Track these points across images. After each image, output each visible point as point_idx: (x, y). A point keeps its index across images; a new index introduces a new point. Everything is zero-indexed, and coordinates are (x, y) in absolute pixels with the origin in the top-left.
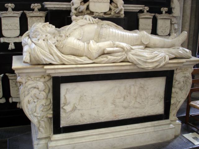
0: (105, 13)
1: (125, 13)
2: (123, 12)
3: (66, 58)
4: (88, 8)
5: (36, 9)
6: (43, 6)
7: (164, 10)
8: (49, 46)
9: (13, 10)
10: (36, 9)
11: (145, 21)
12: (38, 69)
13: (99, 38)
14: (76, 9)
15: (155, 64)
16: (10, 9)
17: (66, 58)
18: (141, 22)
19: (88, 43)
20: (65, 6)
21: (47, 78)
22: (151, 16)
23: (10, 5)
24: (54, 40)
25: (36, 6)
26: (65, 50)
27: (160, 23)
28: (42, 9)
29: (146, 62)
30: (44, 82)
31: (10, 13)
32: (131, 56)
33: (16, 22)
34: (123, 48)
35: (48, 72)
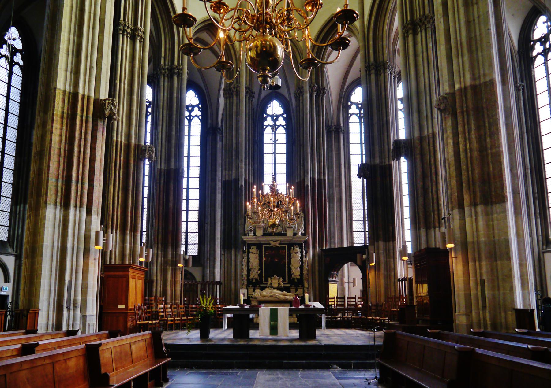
11: (293, 289)
13: (271, 293)
25: (258, 286)
27: (299, 290)
28: (260, 287)
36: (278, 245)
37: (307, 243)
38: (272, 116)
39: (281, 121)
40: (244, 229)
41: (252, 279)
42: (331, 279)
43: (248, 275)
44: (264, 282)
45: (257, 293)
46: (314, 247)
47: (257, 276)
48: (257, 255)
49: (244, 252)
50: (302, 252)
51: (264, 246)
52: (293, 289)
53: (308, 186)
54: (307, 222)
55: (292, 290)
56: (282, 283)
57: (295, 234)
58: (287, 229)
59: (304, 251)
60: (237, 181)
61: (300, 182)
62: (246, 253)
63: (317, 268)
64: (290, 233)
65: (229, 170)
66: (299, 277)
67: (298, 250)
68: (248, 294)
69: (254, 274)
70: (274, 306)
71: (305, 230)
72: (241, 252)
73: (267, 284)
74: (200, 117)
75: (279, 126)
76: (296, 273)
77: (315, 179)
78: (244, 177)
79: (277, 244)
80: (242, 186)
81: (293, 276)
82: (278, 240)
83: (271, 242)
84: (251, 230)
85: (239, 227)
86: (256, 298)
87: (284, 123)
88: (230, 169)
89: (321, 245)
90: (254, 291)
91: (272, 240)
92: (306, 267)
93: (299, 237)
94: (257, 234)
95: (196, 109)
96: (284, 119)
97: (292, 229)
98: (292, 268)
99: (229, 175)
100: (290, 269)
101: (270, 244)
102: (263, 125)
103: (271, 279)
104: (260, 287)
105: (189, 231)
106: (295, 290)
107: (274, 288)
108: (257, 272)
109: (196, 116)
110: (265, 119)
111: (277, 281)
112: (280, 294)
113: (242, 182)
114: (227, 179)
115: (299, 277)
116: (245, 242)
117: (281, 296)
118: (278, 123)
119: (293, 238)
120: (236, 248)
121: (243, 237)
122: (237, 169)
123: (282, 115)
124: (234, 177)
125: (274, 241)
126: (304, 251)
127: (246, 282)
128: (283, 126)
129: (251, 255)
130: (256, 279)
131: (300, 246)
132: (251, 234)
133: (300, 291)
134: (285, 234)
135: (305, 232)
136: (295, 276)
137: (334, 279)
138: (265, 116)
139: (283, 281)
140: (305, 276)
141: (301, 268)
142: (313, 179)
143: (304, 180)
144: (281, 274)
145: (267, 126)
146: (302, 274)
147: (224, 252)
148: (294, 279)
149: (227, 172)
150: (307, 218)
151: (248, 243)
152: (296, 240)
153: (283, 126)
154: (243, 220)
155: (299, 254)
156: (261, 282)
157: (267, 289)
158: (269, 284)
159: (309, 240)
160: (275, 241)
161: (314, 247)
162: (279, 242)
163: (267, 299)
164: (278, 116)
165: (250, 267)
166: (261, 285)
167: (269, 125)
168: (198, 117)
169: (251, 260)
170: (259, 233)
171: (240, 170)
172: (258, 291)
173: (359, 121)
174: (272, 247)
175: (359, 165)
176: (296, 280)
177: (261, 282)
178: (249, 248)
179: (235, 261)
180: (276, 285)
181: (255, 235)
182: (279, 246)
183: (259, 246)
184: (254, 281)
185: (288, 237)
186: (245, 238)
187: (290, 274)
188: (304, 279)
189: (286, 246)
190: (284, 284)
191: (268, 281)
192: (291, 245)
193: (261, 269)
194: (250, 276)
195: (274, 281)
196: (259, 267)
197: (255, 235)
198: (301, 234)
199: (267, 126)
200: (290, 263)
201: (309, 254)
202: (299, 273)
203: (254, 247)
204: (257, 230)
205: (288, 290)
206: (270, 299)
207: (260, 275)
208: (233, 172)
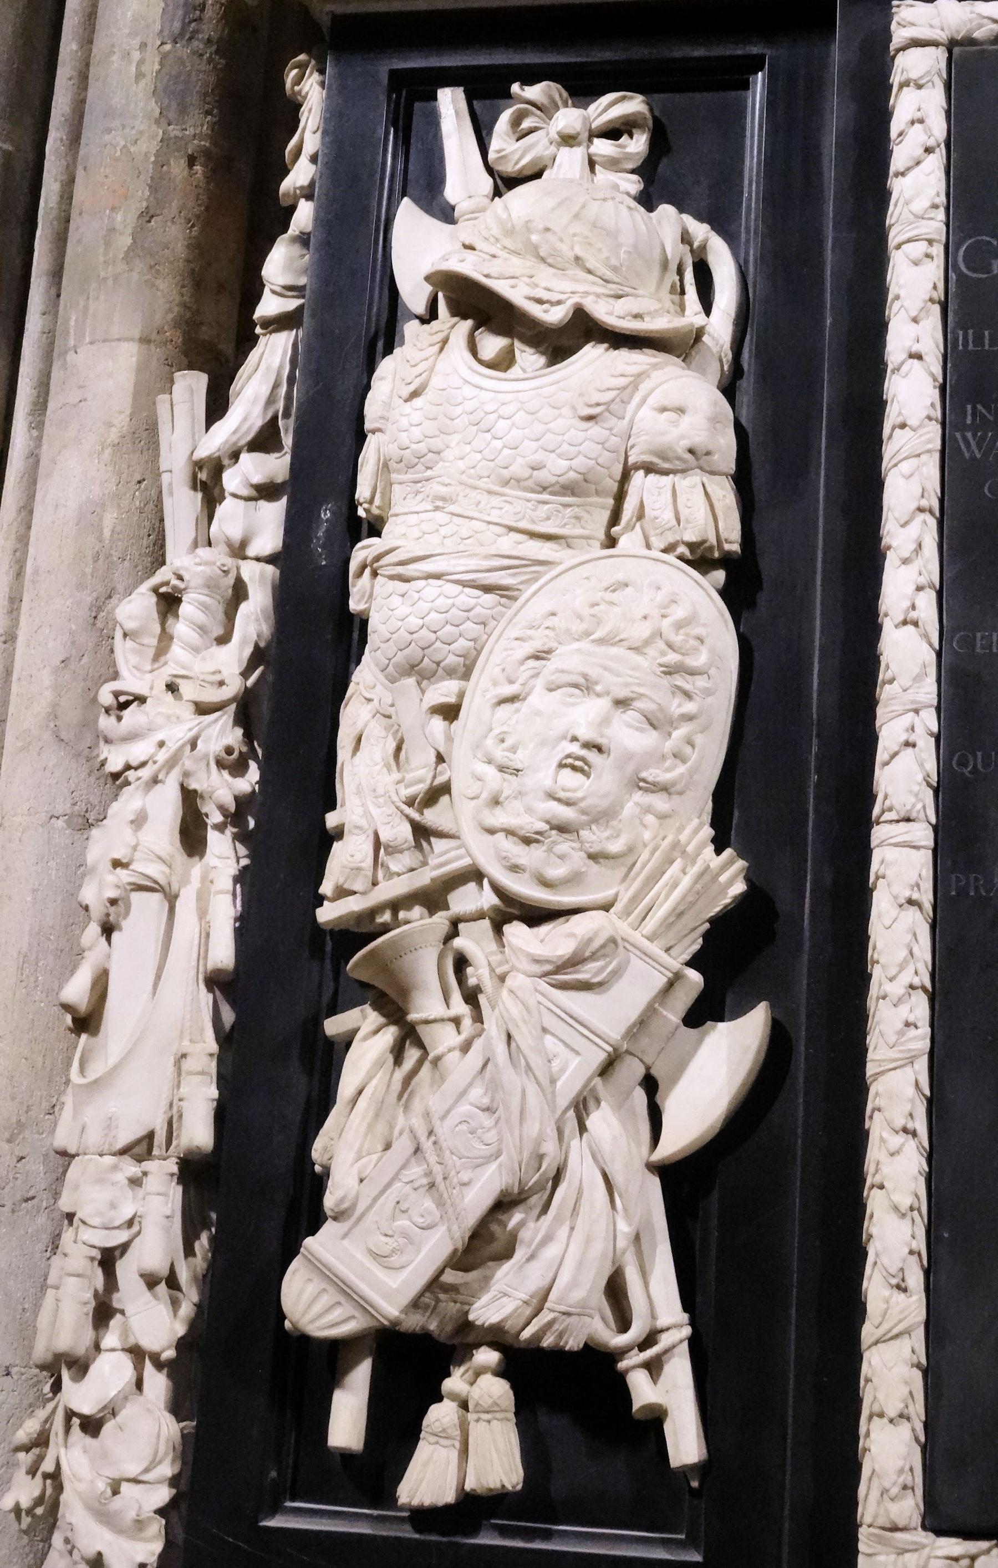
41: (411, 1365)
43: (255, 1189)
47: (599, 1261)
48: (686, 408)
49: (212, 343)
130: (567, 1389)
165: (350, 881)
193: (777, 947)
194: (302, 1204)
207: (762, 1211)
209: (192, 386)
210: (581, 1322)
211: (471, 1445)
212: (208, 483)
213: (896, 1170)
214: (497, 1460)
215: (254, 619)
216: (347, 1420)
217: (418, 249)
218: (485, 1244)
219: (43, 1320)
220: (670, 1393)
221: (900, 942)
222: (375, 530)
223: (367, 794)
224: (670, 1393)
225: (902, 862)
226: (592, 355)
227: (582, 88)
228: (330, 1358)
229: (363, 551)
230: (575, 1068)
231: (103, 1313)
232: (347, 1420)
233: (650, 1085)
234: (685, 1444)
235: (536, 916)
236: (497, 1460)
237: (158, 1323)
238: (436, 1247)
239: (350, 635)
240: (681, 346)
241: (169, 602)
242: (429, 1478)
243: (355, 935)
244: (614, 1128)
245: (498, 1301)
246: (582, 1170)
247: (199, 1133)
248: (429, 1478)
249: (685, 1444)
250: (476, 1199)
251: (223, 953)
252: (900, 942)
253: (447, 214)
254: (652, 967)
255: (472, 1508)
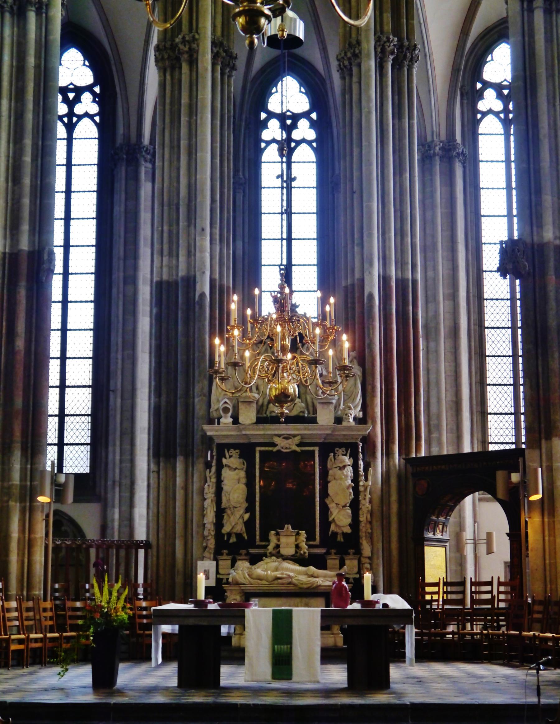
0: (293, 556)
1: (309, 554)
2: (307, 554)
3: (252, 581)
4: (279, 552)
5: (243, 554)
6: (248, 551)
7: (352, 551)
8: (244, 574)
9: (227, 554)
10: (243, 554)
11: (333, 561)
12: (237, 588)
13: (277, 569)
14: (270, 553)
15: (309, 585)
16: (225, 554)
17: (252, 581)
18: (329, 562)
19: (267, 572)
20: (263, 551)
21: (242, 594)
22: (338, 557)
23: (225, 551)
24: (247, 571)
25: (243, 552)
26: (254, 576)
27: (347, 562)
28: (248, 554)
29: (302, 584)
30: (241, 597)
31: (225, 557)
32: (294, 580)
33: (229, 562)
34: (289, 575)
35: (242, 588)
36: (295, 448)
37: (368, 441)
38: (282, 117)
39: (304, 131)
40: (209, 406)
41: (229, 535)
42: (430, 535)
44: (258, 543)
45: (242, 571)
46: (388, 453)
47: (240, 528)
48: (242, 474)
49: (208, 465)
50: (355, 466)
51: (258, 449)
52: (333, 561)
53: (371, 296)
54: (369, 388)
55: (330, 562)
56: (304, 546)
57: (338, 420)
58: (319, 408)
59: (361, 463)
60: (190, 282)
61: (353, 285)
62: (214, 469)
63: (394, 507)
64: (325, 417)
65: (170, 255)
66: (348, 530)
67: (347, 460)
68: (217, 572)
69: (235, 523)
70: (282, 605)
71: (364, 407)
72: (199, 466)
73: (266, 547)
74: (97, 119)
75: (298, 143)
76: (341, 519)
77: (390, 278)
78: (208, 274)
79: (292, 445)
80: (203, 295)
81: (333, 527)
82: (295, 436)
83: (277, 440)
84: (226, 410)
85: (196, 400)
86: (237, 584)
87: (311, 135)
88: (173, 253)
89: (405, 448)
90: (233, 566)
91: (279, 436)
92: (365, 505)
93: (349, 428)
94: (241, 420)
95: (87, 97)
96: (313, 125)
97: (332, 407)
98: (332, 506)
99: (170, 267)
100: (325, 509)
101: (274, 445)
102: (259, 140)
103: (278, 534)
104: (248, 554)
105: (67, 412)
106: (337, 562)
107: (285, 558)
108: (242, 517)
109: (86, 115)
110: (264, 125)
111: (292, 539)
112: (300, 573)
113: (202, 286)
114: (165, 277)
115: (348, 530)
116: (211, 439)
117: (304, 579)
118: (296, 135)
119: (334, 430)
120: (189, 455)
121: (206, 427)
122: (190, 253)
123: (306, 115)
124: (182, 272)
125: (286, 438)
126: (361, 463)
127: (212, 543)
128: (309, 143)
129: (226, 473)
130: (239, 536)
131: (351, 448)
132: (227, 420)
133: (351, 565)
134: (313, 421)
135: (365, 414)
136: (337, 525)
137: (438, 536)
138: (263, 116)
139: (308, 539)
140: (364, 527)
141: (355, 505)
142: (385, 280)
143: (362, 281)
144: (303, 522)
145: (268, 143)
146: (355, 523)
147: (158, 464)
148: (335, 534)
149: (165, 259)
150: (369, 378)
151: (217, 441)
152: (341, 434)
153: (309, 143)
154: (206, 383)
155: (349, 471)
156: (251, 543)
157: (266, 560)
158: (271, 548)
159: (375, 435)
160: (287, 437)
161: (388, 453)
162: (297, 440)
163: (264, 586)
164: (296, 118)
165: (223, 506)
166: (252, 551)
167: (274, 141)
168: (91, 117)
169: (227, 486)
170: (248, 416)
171: (198, 254)
172: (243, 565)
173: (502, 131)
174: (279, 452)
175: (501, 243)
176: (340, 539)
177: (251, 543)
178: (221, 455)
179: (186, 488)
180: (288, 550)
181: (236, 421)
182: (298, 449)
183: (246, 450)
184: (233, 540)
185: (323, 428)
186: (210, 430)
187: (326, 522)
188: (362, 534)
189: (317, 449)
190: (310, 546)
191: (268, 541)
192: (328, 448)
193: (250, 509)
194: (222, 526)
195: (283, 540)
196: (245, 505)
197: (236, 421)
198: (355, 419)
199: (268, 143)
200: (324, 493)
201: (375, 470)
202: (349, 520)
203: (235, 453)
204: (242, 407)
205: (320, 563)
206: (276, 587)
207: (249, 525)
208: (182, 258)
209: (208, 470)
210: (239, 532)
211: (233, 540)
212: (210, 478)
213: (258, 522)
214: (235, 540)
215: (214, 488)
216: (226, 539)
217: (224, 461)
218: (233, 528)
219: (205, 533)
220: (245, 536)
221: (258, 509)
222: (223, 481)
223: (224, 499)
224: (245, 536)
225: (257, 504)
226: (237, 471)
227: (235, 450)
228: (224, 535)
229: (222, 483)
230: (238, 516)
231: (209, 533)
232: (226, 539)
233: (243, 517)
234: (246, 538)
235: (236, 507)
236: (235, 540)
237: (213, 533)
238: (230, 528)
239: (222, 489)
240: (242, 469)
241: (209, 486)
242: (231, 541)
243: (224, 509)
244: (241, 520)
245: (235, 530)
246: (239, 523)
247: (215, 522)
248: (231, 541)
249: (246, 538)
250: (233, 524)
251: (215, 510)
252: (258, 509)
253: (226, 458)
254: (242, 511)
255: (234, 543)
